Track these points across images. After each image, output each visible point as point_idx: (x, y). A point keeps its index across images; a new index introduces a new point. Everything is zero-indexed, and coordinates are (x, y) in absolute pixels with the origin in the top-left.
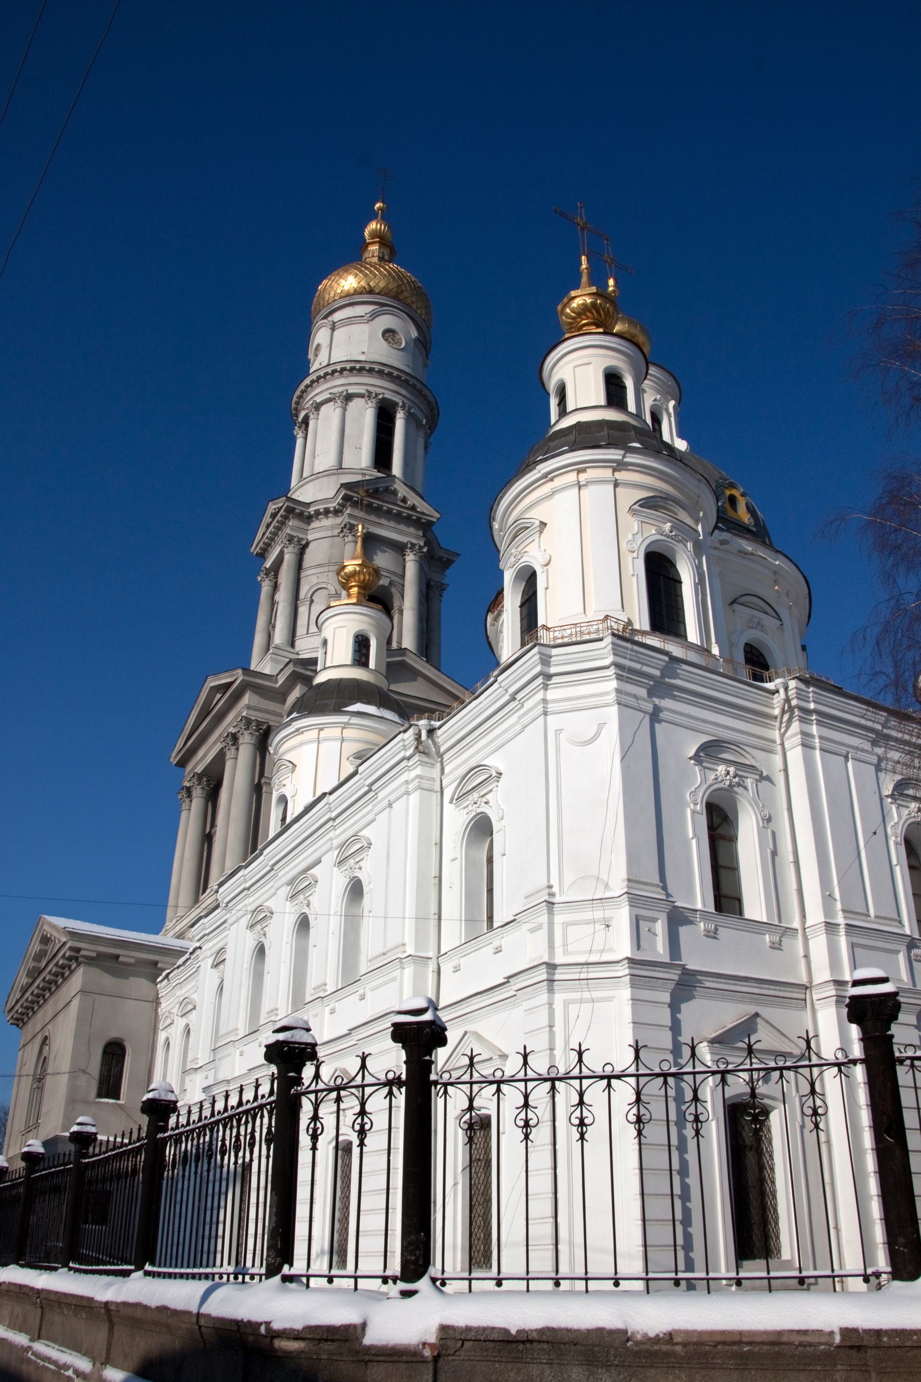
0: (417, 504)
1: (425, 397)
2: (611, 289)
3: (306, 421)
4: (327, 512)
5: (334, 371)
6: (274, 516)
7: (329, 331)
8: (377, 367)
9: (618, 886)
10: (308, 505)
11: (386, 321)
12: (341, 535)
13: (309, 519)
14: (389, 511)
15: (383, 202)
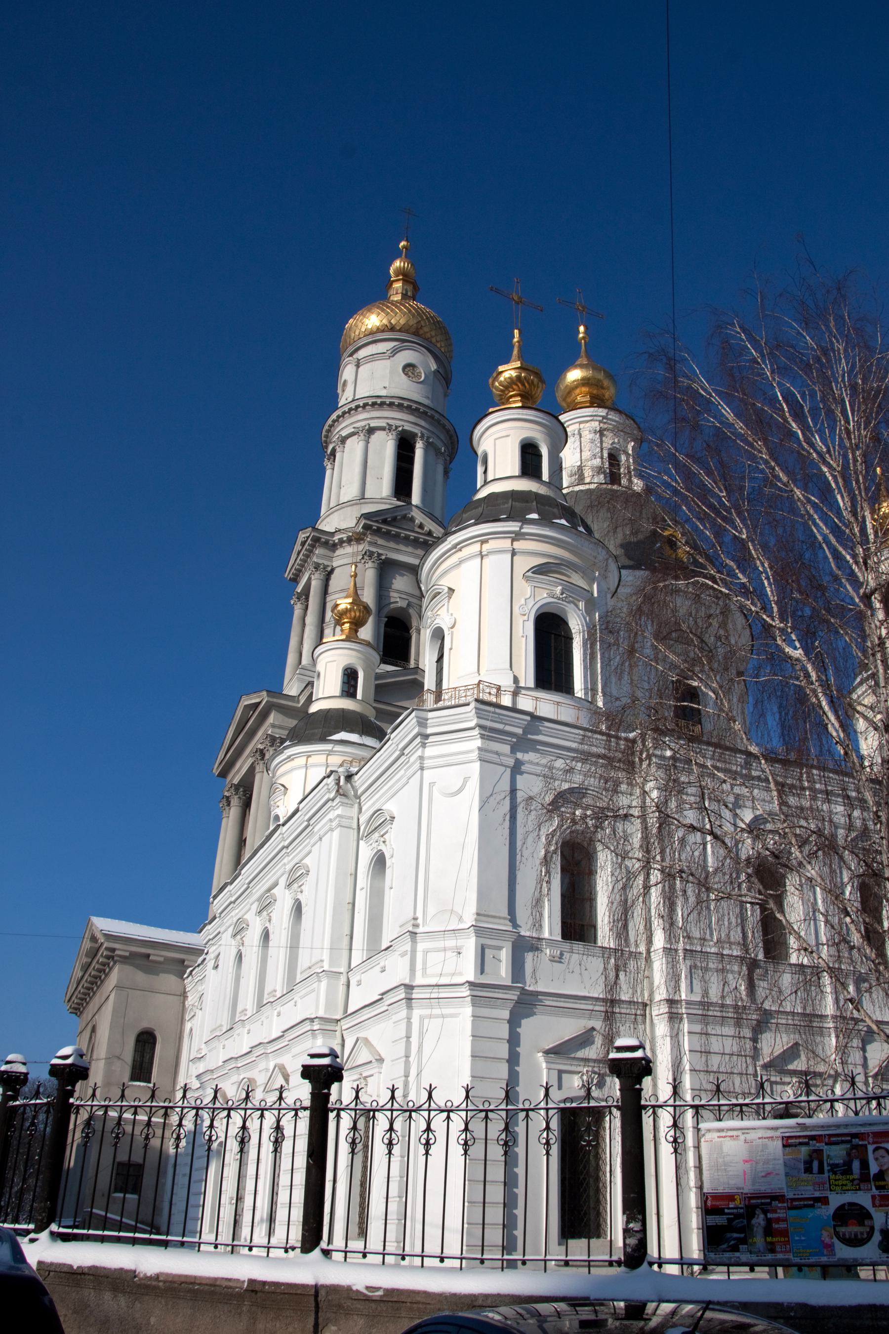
0: (433, 529)
1: (444, 426)
2: (581, 335)
3: (333, 453)
5: (357, 407)
6: (303, 544)
7: (355, 368)
8: (397, 402)
9: (469, 919)
10: (332, 534)
12: (363, 561)
13: (334, 547)
14: (407, 538)
15: (407, 241)
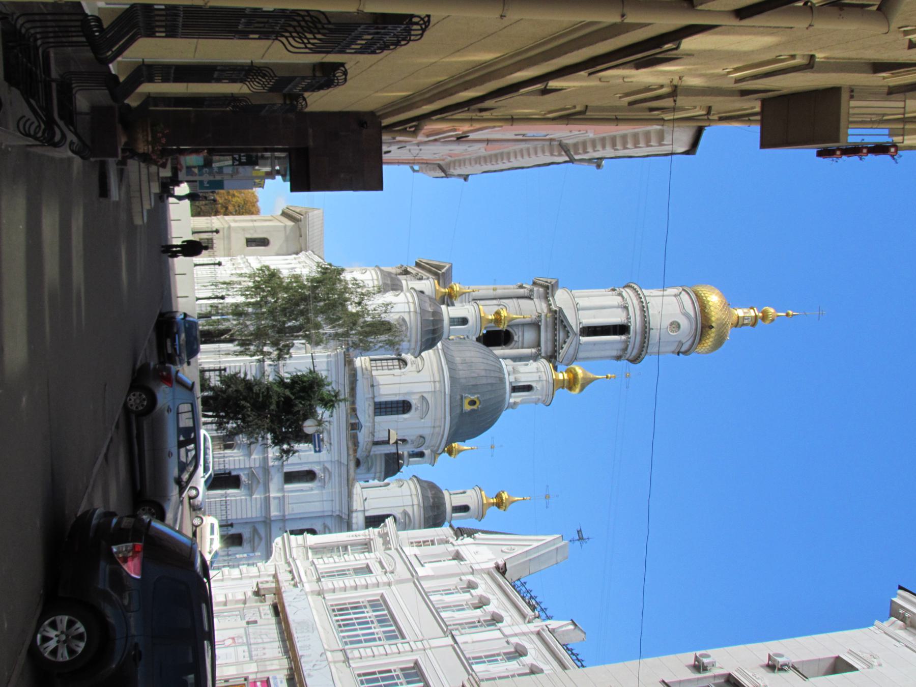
4: (551, 305)
5: (641, 298)
7: (674, 294)
10: (553, 296)
11: (684, 323)
13: (546, 298)
